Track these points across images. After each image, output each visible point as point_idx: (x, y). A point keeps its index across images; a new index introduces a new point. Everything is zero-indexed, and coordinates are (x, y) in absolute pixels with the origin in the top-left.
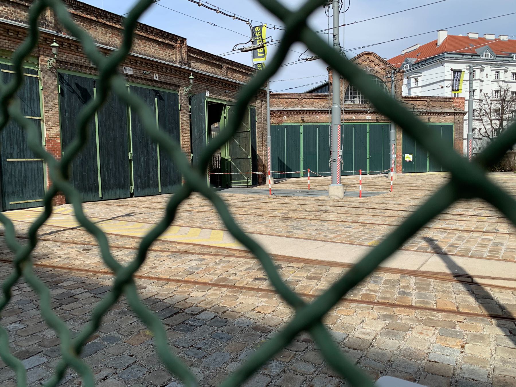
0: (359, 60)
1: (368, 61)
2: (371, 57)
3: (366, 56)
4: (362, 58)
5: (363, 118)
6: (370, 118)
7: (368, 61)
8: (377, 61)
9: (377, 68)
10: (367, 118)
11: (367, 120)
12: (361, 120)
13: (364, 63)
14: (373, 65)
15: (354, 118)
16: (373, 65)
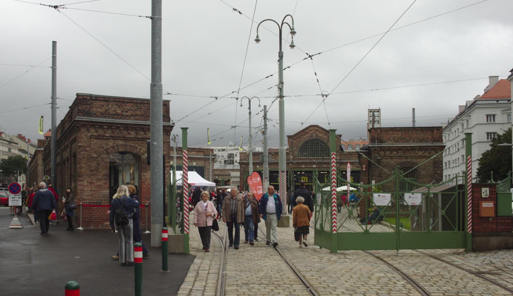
0: (307, 130)
1: (314, 131)
2: (316, 128)
3: (312, 128)
4: (309, 129)
5: (311, 167)
6: (315, 167)
7: (314, 131)
8: (321, 130)
9: (321, 135)
10: (313, 167)
11: (313, 168)
12: (309, 168)
13: (311, 132)
14: (318, 133)
15: (303, 166)
16: (317, 133)
